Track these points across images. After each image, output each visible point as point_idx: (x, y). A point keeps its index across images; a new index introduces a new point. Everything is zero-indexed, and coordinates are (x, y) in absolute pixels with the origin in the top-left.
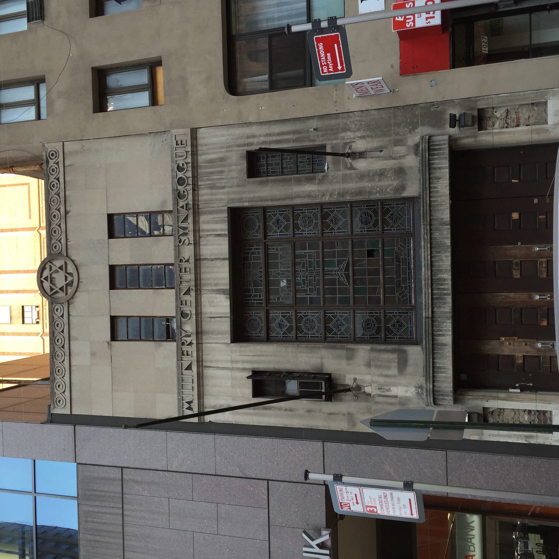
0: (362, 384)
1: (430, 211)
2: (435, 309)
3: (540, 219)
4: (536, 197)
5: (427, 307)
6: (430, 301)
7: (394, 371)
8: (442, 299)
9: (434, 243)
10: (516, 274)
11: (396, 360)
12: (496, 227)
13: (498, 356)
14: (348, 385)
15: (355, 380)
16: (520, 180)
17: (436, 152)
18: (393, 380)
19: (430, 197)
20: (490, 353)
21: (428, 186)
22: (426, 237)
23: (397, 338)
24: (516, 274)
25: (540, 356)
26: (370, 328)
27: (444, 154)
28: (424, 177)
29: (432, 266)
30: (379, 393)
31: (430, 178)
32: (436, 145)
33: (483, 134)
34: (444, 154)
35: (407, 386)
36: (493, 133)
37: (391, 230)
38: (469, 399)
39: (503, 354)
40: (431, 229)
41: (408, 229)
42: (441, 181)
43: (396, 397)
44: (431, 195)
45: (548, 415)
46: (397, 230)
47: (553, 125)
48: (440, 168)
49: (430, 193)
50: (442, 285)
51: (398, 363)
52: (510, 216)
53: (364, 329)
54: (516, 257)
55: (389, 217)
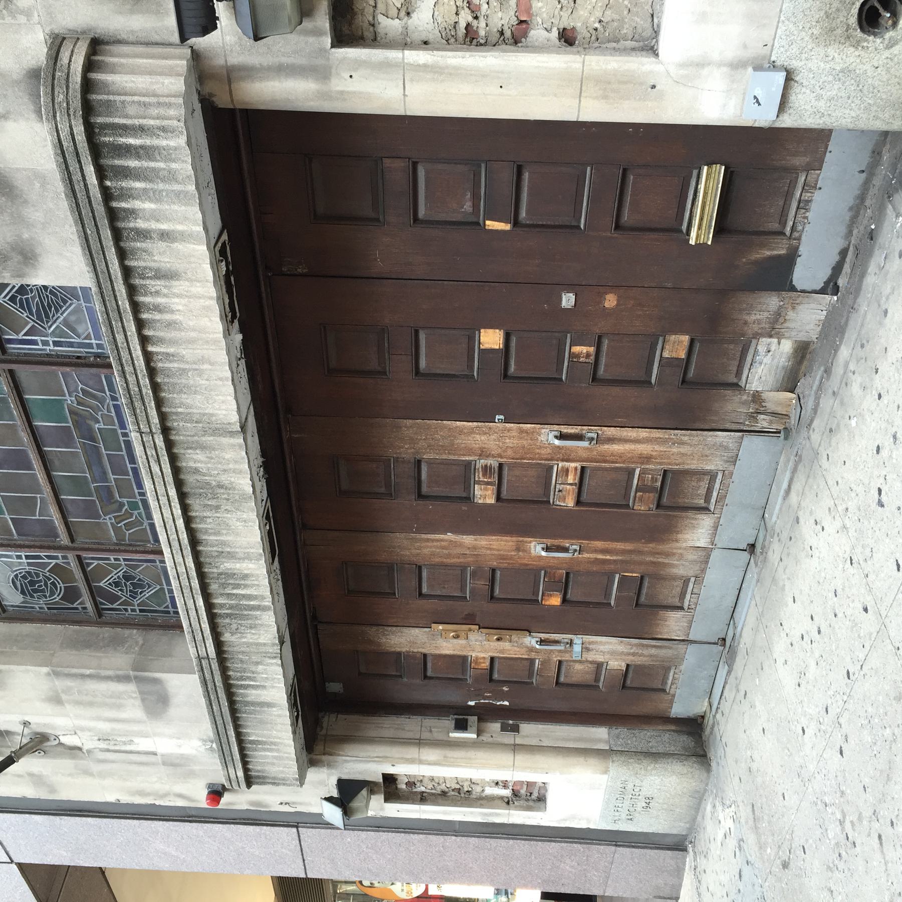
0: (49, 731)
1: (156, 388)
2: (227, 637)
3: (578, 356)
4: (570, 287)
5: (199, 637)
6: (206, 626)
7: (134, 710)
8: (247, 617)
9: (190, 479)
10: (484, 495)
11: (137, 695)
12: (423, 364)
13: (425, 655)
14: (8, 733)
15: (26, 724)
16: (516, 223)
17: (133, 163)
18: (135, 728)
19: (144, 341)
20: (404, 650)
21: (125, 304)
22: (156, 469)
23: (133, 610)
24: (484, 495)
25: (535, 659)
26: (43, 591)
27: (171, 177)
28: (101, 266)
29: (194, 542)
30: (103, 745)
31: (127, 272)
32: (125, 129)
33: (359, 64)
34: (171, 177)
35: (179, 738)
36: (402, 66)
37: (34, 343)
38: (346, 761)
39: (437, 652)
40: (170, 445)
41: (99, 346)
42: (179, 286)
43: (155, 754)
44: (147, 332)
45: (541, 804)
46: (56, 344)
47: (682, 65)
48: (165, 236)
49: (140, 325)
50: (237, 586)
51: (143, 700)
52: (472, 339)
53: (23, 592)
54: (483, 453)
55: (13, 299)
